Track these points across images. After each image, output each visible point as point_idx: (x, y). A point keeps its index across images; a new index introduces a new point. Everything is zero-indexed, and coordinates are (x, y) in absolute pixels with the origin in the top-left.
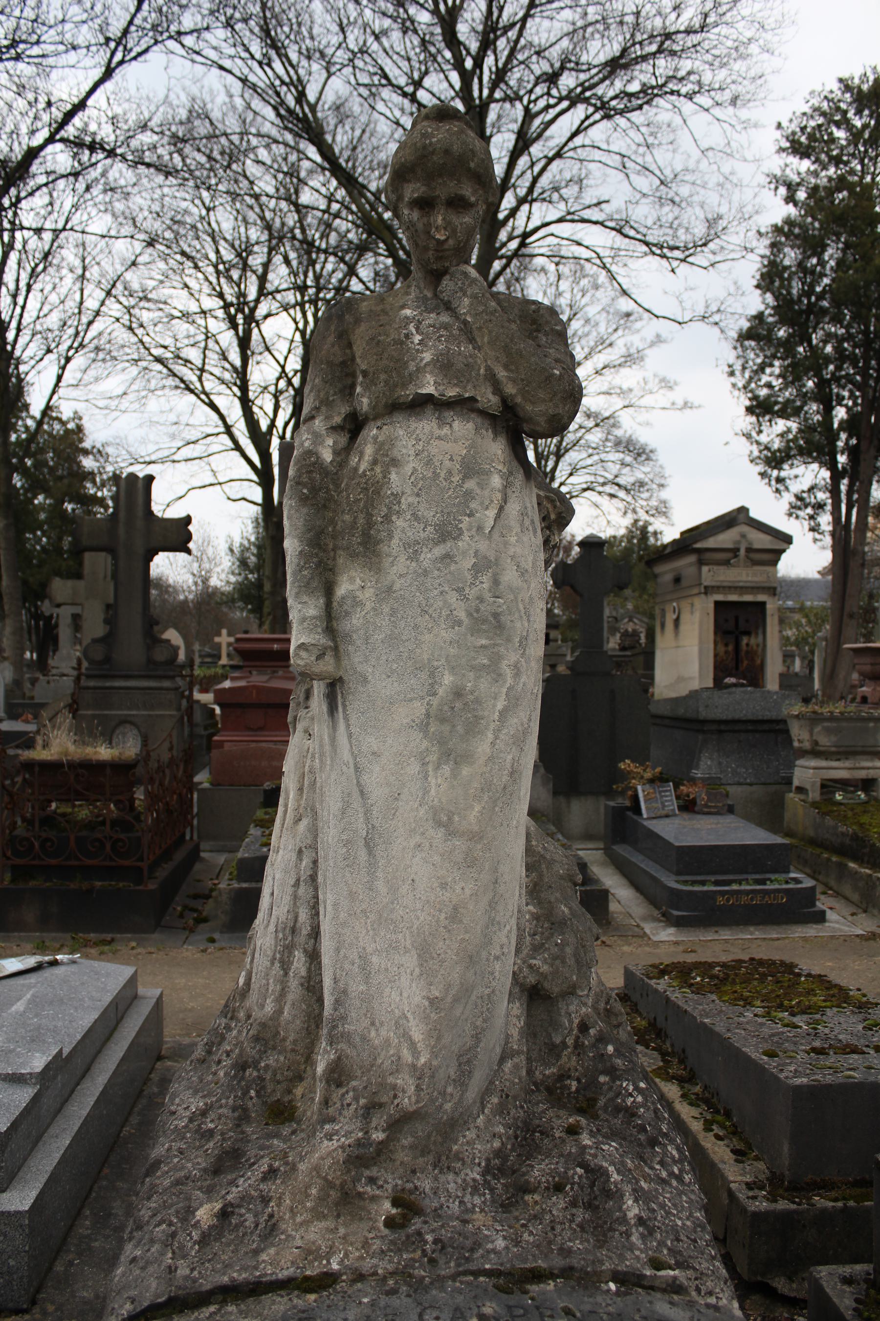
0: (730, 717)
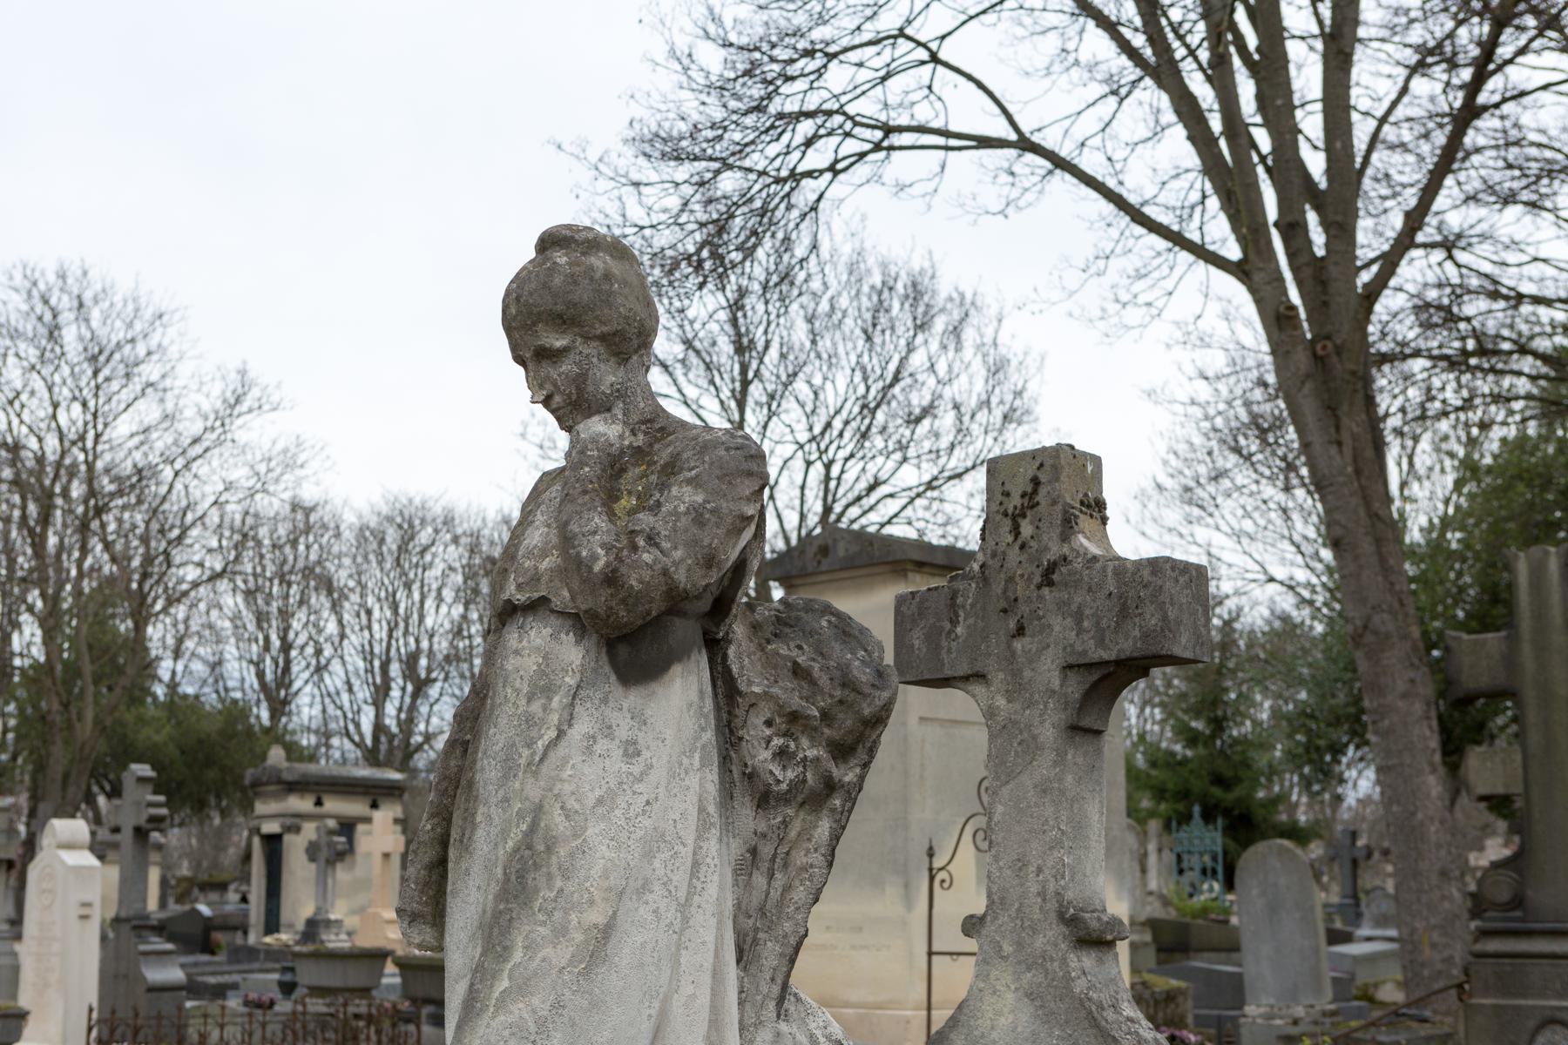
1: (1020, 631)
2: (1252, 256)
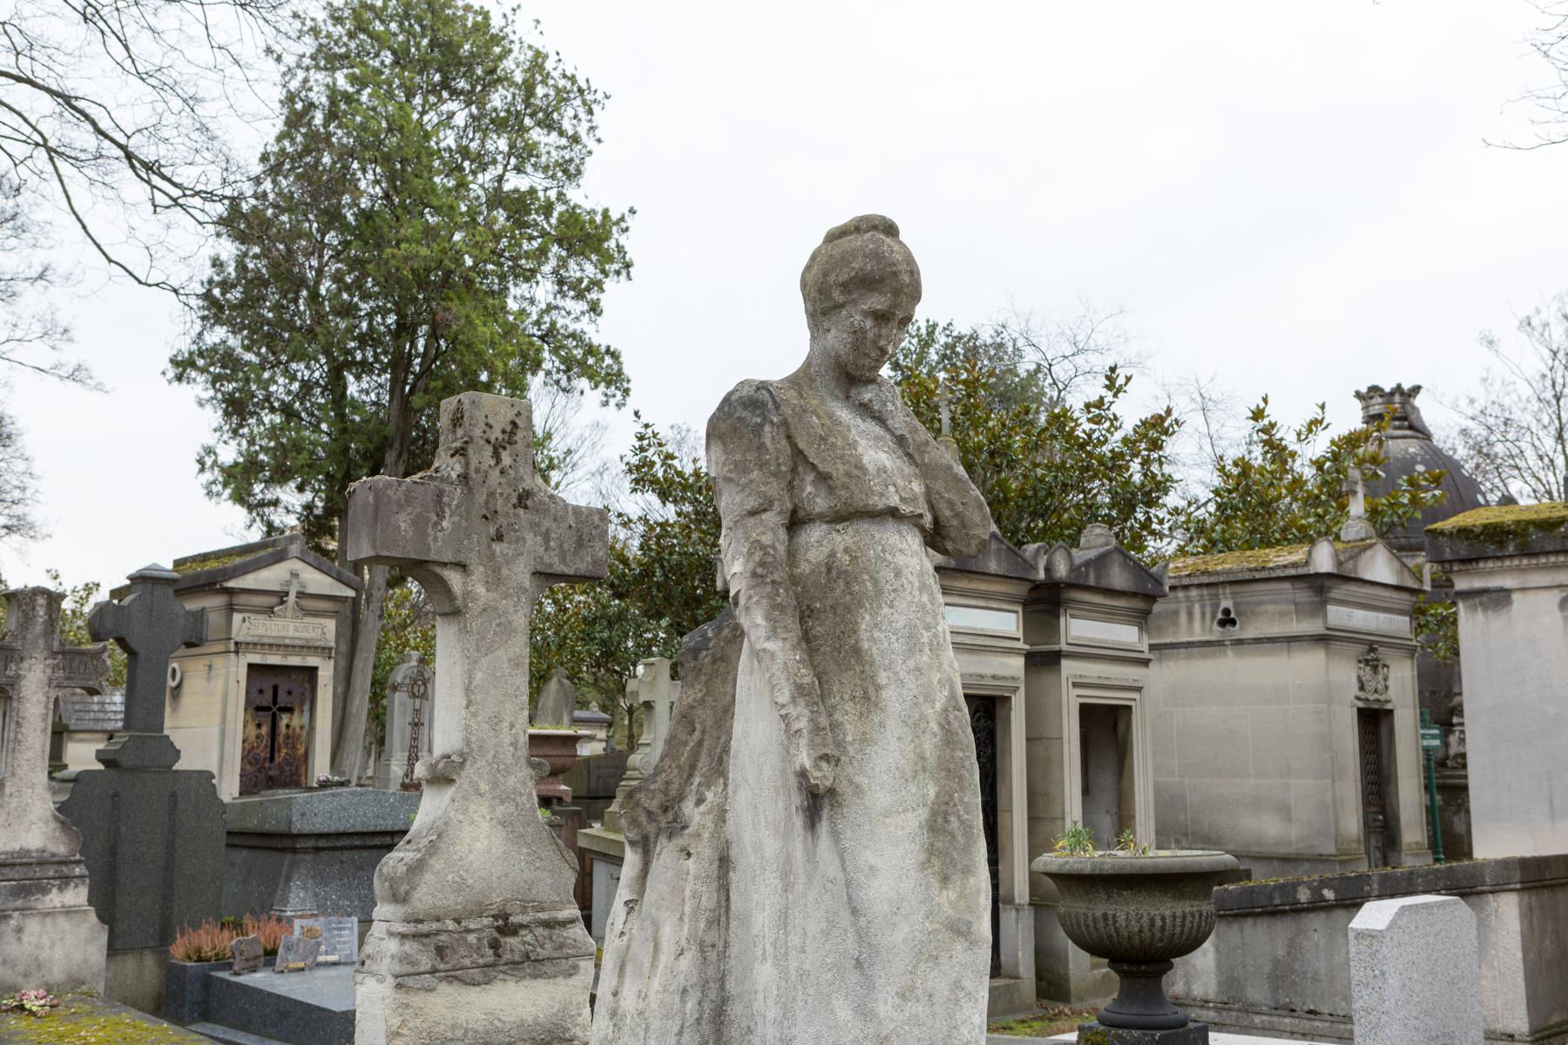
0: (333, 829)
1: (499, 538)
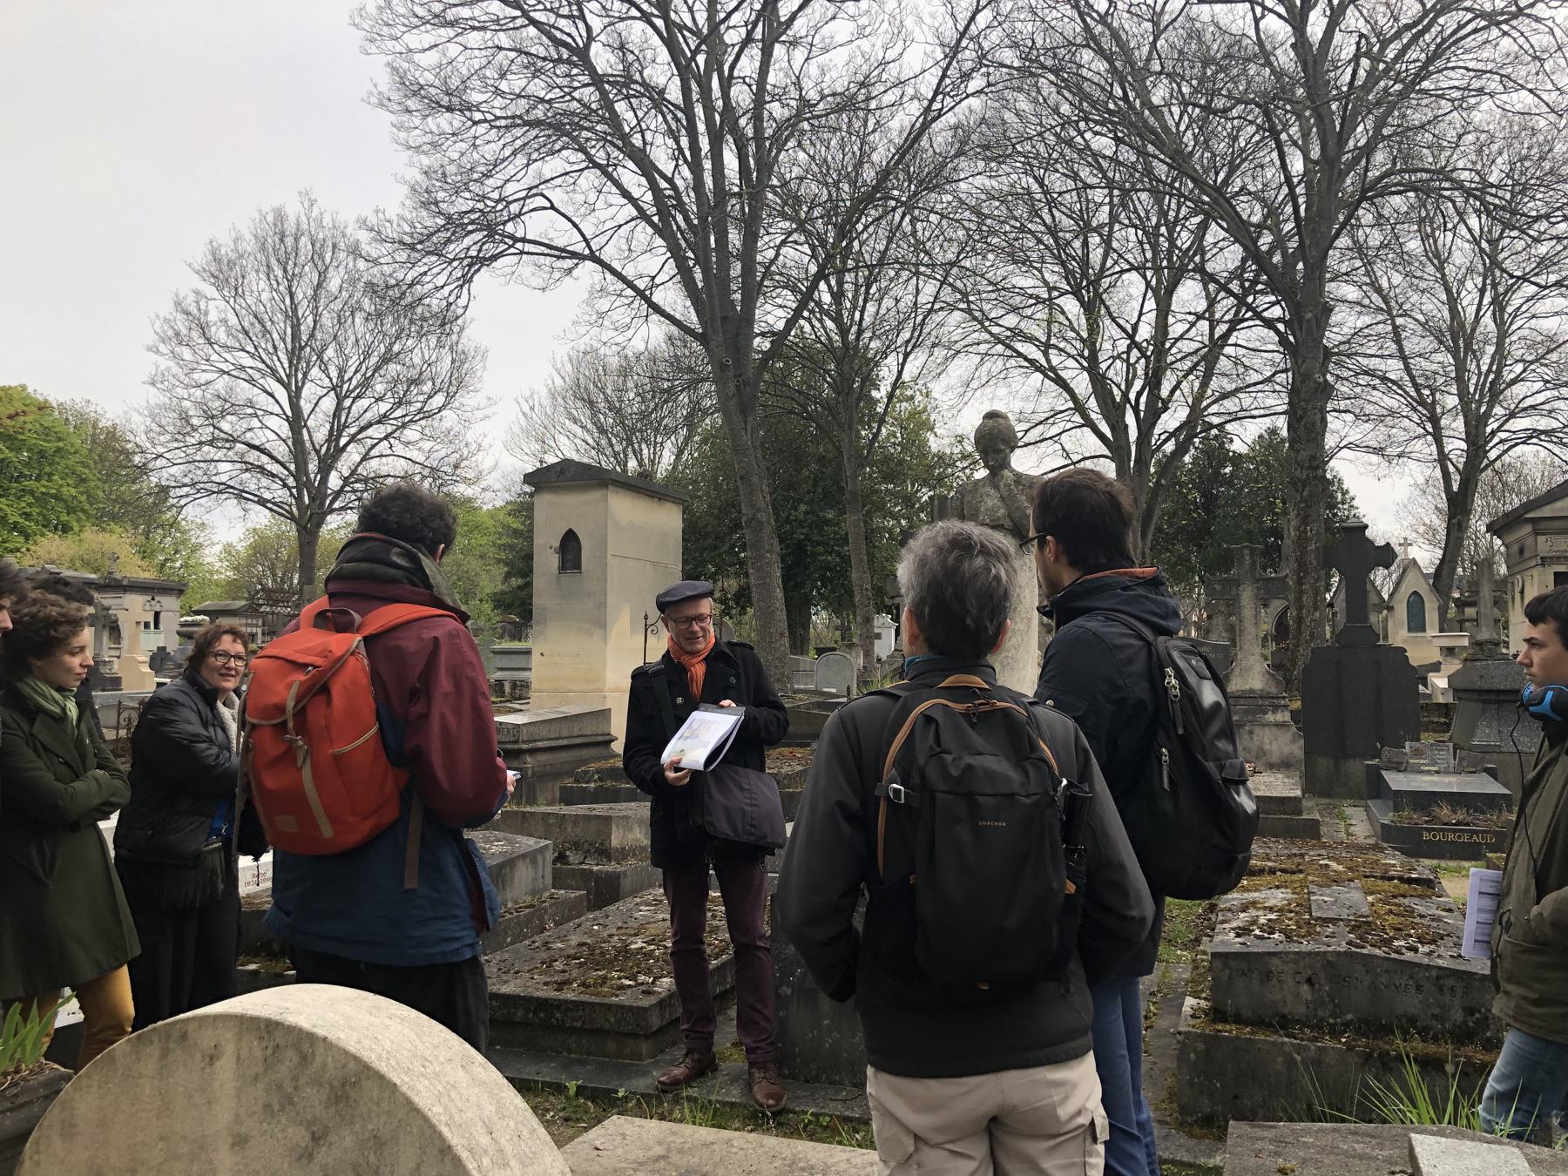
2: (710, 332)
